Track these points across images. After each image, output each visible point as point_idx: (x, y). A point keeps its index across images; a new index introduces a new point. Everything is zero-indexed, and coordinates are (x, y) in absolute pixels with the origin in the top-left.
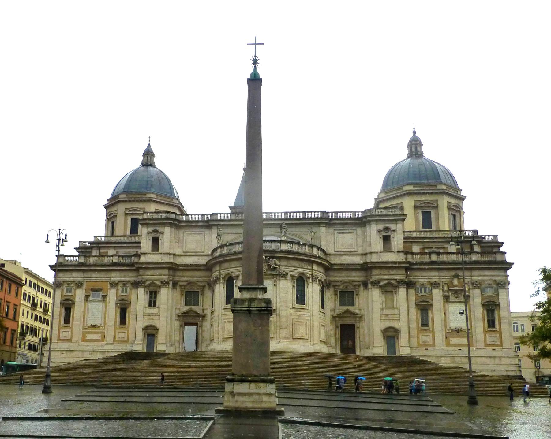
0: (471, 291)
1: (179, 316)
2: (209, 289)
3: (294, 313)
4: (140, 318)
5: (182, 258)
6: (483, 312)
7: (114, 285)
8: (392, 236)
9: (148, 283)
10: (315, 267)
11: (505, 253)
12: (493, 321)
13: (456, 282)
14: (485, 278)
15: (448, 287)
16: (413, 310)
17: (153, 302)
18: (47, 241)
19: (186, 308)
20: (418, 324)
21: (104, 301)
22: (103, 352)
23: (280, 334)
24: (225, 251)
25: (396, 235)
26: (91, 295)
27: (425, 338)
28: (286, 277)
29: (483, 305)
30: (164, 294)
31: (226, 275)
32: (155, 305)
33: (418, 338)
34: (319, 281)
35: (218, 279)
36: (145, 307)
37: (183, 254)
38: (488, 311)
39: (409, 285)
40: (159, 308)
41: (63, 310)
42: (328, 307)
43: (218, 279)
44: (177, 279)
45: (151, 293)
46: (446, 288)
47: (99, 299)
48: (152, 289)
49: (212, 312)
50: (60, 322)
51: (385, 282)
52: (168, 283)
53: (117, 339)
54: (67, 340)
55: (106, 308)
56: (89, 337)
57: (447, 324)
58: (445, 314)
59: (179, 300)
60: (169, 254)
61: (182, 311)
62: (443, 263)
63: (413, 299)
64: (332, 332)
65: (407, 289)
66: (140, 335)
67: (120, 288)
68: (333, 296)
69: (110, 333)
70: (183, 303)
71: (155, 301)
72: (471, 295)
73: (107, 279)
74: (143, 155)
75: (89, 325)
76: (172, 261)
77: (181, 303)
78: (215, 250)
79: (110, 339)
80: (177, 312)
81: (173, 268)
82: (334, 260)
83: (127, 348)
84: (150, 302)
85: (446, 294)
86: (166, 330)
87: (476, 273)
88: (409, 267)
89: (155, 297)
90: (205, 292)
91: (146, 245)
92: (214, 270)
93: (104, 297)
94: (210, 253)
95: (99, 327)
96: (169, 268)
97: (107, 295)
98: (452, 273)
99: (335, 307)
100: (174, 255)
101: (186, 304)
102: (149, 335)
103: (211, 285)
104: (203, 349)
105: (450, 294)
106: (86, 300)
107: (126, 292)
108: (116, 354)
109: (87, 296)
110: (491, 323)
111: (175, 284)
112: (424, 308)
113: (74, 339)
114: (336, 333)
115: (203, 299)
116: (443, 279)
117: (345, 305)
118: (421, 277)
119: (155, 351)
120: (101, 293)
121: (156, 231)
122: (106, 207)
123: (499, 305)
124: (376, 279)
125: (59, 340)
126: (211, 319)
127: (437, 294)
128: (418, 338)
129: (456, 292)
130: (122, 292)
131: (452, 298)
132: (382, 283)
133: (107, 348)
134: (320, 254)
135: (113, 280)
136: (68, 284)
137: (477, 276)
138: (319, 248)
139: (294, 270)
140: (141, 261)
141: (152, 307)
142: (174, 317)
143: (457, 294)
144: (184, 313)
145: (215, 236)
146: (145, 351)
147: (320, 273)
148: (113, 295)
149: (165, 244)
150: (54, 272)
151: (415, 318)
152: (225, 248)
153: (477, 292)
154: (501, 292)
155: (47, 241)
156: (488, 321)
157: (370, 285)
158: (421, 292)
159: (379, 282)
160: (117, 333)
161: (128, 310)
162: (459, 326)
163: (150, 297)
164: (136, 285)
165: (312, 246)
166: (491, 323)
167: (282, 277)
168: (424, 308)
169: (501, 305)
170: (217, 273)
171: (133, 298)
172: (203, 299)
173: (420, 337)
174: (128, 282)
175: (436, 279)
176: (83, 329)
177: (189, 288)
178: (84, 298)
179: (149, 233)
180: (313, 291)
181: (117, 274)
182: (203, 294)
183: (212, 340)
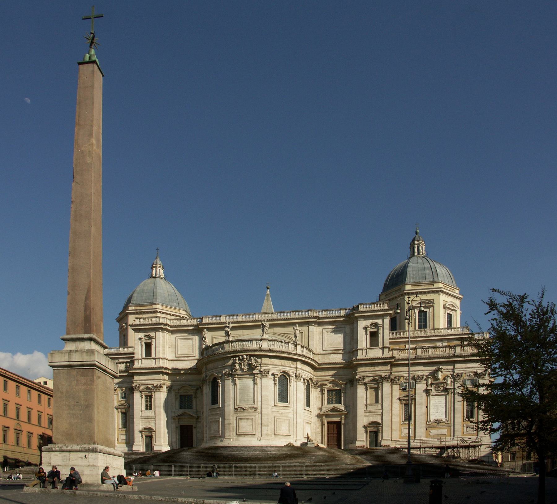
10: (299, 365)
14: (467, 370)
19: (181, 411)
34: (304, 379)
39: (393, 381)
42: (315, 406)
45: (146, 396)
51: (371, 378)
61: (176, 415)
64: (319, 430)
70: (178, 406)
71: (151, 405)
77: (175, 406)
82: (320, 359)
85: (429, 388)
87: (457, 366)
88: (392, 363)
89: (151, 401)
99: (322, 405)
101: (181, 408)
117: (332, 403)
121: (149, 337)
124: (362, 375)
132: (367, 380)
134: (305, 352)
139: (276, 367)
147: (306, 372)
157: (355, 382)
159: (364, 379)
162: (439, 418)
163: (147, 401)
165: (296, 345)
168: (408, 403)
177: (182, 392)
182: (196, 397)
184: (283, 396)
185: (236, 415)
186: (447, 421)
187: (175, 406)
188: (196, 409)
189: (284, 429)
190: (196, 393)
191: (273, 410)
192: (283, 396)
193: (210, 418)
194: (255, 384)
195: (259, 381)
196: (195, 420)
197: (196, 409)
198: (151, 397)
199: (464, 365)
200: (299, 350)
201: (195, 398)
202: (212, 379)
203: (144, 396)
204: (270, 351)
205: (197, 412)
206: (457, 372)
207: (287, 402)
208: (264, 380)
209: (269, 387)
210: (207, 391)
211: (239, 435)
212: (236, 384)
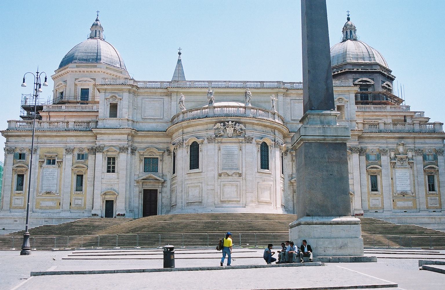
1: (138, 182)
2: (169, 154)
3: (259, 177)
5: (141, 124)
6: (425, 178)
7: (69, 151)
11: (443, 124)
12: (433, 186)
13: (401, 149)
15: (395, 154)
17: (111, 168)
20: (368, 190)
22: (60, 219)
23: (246, 197)
25: (349, 105)
28: (251, 143)
29: (425, 171)
32: (113, 171)
33: (369, 201)
35: (181, 144)
37: (142, 121)
38: (429, 177)
39: (361, 151)
44: (136, 145)
45: (109, 159)
46: (393, 155)
48: (111, 154)
52: (127, 149)
53: (73, 205)
54: (21, 208)
57: (395, 188)
59: (138, 167)
61: (141, 178)
63: (364, 164)
65: (359, 155)
68: (291, 163)
70: (142, 169)
71: (114, 167)
73: (62, 145)
77: (140, 169)
79: (66, 206)
80: (136, 177)
84: (109, 168)
86: (126, 197)
87: (417, 141)
89: (114, 163)
90: (164, 159)
91: (104, 110)
92: (174, 136)
97: (62, 162)
98: (397, 141)
99: (292, 173)
106: (41, 167)
111: (133, 151)
114: (293, 197)
115: (162, 165)
116: (391, 146)
126: (171, 185)
128: (369, 201)
129: (402, 159)
131: (398, 163)
133: (63, 215)
140: (97, 127)
141: (111, 174)
142: (134, 184)
144: (143, 179)
145: (174, 103)
149: (123, 111)
150: (5, 139)
156: (429, 185)
160: (73, 200)
161: (84, 177)
163: (109, 163)
164: (94, 150)
166: (432, 188)
167: (248, 142)
170: (180, 138)
172: (162, 165)
173: (370, 200)
174: (84, 148)
175: (384, 146)
176: (38, 196)
180: (275, 158)
181: (74, 139)
182: (162, 160)
183: (173, 206)
185: (219, 180)
186: (413, 193)
187: (140, 169)
188: (162, 173)
190: (162, 156)
192: (265, 164)
193: (188, 182)
196: (161, 184)
197: (162, 173)
198: (114, 159)
199: (422, 141)
201: (161, 160)
202: (190, 144)
203: (107, 158)
205: (163, 175)
208: (248, 146)
209: (253, 151)
210: (183, 156)
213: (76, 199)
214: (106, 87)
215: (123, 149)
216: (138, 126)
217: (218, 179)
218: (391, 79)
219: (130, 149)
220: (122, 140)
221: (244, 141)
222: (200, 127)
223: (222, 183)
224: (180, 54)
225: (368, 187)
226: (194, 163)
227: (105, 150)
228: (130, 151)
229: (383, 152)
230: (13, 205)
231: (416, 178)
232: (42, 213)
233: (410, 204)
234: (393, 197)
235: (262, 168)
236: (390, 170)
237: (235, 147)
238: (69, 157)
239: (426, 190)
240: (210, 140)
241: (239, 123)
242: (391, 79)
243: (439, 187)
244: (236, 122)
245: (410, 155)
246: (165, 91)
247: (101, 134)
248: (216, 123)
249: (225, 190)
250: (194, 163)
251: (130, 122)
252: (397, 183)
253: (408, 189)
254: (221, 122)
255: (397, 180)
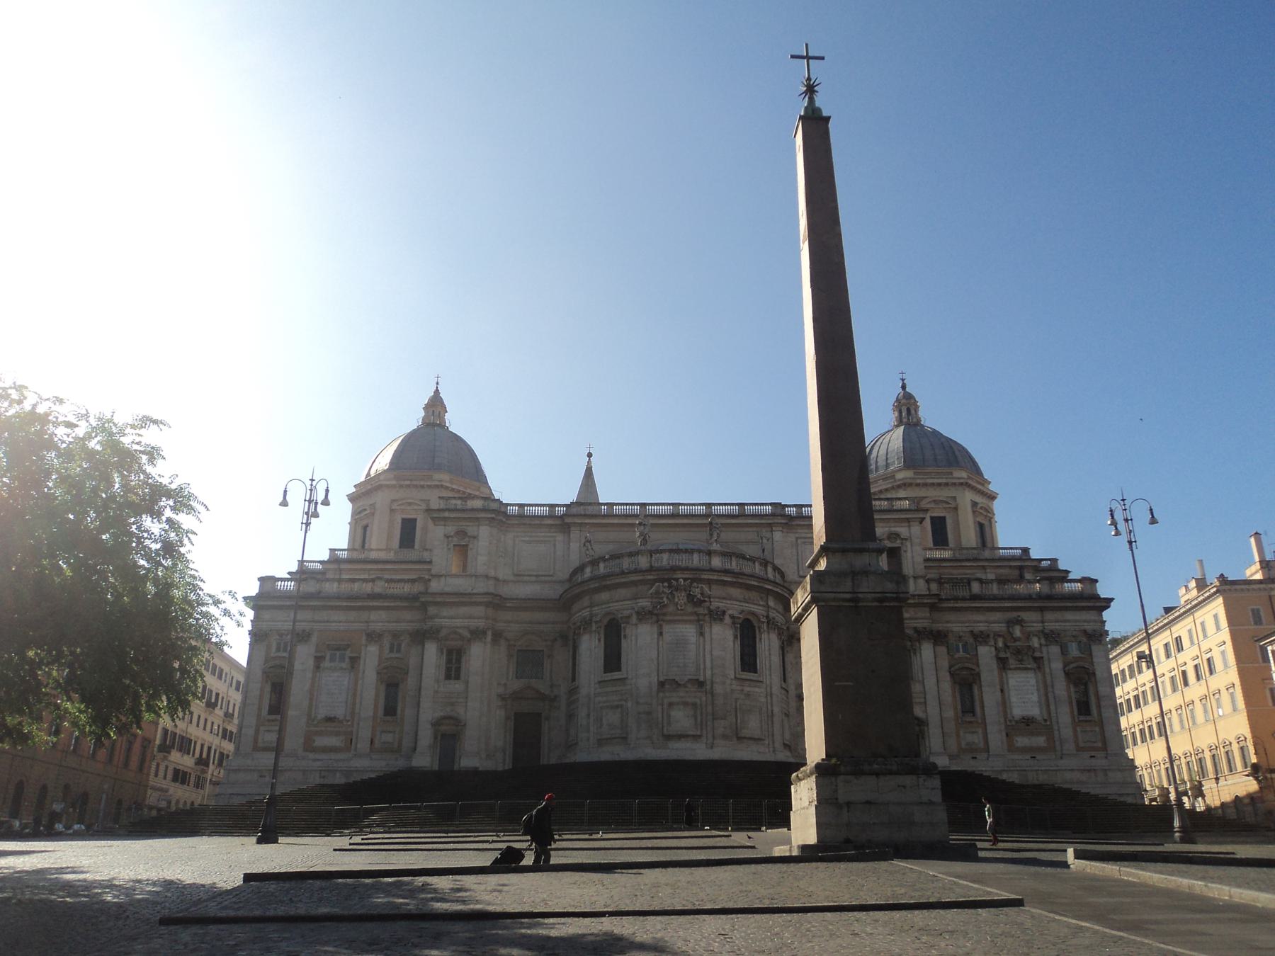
0: (1044, 649)
4: (426, 704)
7: (373, 637)
8: (904, 548)
9: (444, 633)
11: (1096, 581)
13: (1017, 632)
16: (947, 685)
18: (284, 503)
19: (516, 685)
21: (353, 667)
24: (602, 569)
26: (328, 658)
27: (969, 738)
29: (1067, 674)
30: (478, 657)
31: (608, 614)
32: (457, 677)
33: (958, 736)
35: (587, 623)
36: (437, 681)
37: (512, 578)
39: (938, 637)
40: (467, 682)
41: (268, 688)
43: (587, 623)
45: (450, 652)
46: (1000, 644)
47: (344, 665)
49: (573, 691)
50: (260, 709)
52: (484, 633)
53: (377, 744)
55: (356, 684)
56: (320, 741)
58: (1002, 691)
60: (487, 577)
62: (995, 598)
63: (945, 664)
65: (935, 645)
66: (426, 737)
67: (386, 642)
69: (365, 733)
71: (458, 670)
72: (1045, 655)
74: (426, 408)
75: (319, 717)
76: (492, 590)
78: (581, 569)
79: (363, 746)
80: (501, 690)
81: (497, 602)
83: (398, 764)
84: (448, 670)
85: (1002, 655)
87: (1049, 616)
89: (459, 661)
91: (443, 559)
92: (576, 607)
93: (354, 661)
94: (567, 576)
95: (341, 722)
96: (487, 605)
97: (358, 658)
100: (496, 579)
102: (443, 736)
103: (569, 640)
104: (553, 761)
105: (1008, 655)
106: (317, 667)
107: (399, 651)
108: (373, 776)
109: (319, 659)
110: (1083, 707)
111: (497, 636)
112: (966, 682)
113: (288, 745)
116: (997, 627)
118: (957, 624)
119: (456, 768)
120: (348, 653)
121: (461, 533)
122: (352, 498)
123: (1094, 674)
125: (256, 748)
127: (985, 653)
128: (958, 736)
129: (1018, 652)
130: (391, 651)
135: (373, 627)
136: (281, 635)
137: (1054, 621)
138: (775, 568)
141: (452, 682)
143: (1017, 655)
145: (575, 546)
146: (436, 767)
148: (371, 656)
151: (950, 699)
152: (602, 565)
153: (1055, 649)
154: (1095, 648)
155: (284, 503)
156: (1078, 703)
158: (958, 651)
163: (449, 661)
164: (420, 637)
165: (765, 563)
169: (1098, 673)
170: (586, 613)
171: (413, 662)
175: (982, 627)
178: (311, 662)
179: (447, 537)
181: (383, 615)
184: (749, 661)
189: (753, 725)
191: (734, 687)
192: (749, 661)
194: (702, 634)
195: (707, 629)
199: (1058, 615)
200: (770, 574)
202: (605, 621)
204: (726, 572)
205: (552, 686)
206: (1050, 626)
207: (755, 671)
210: (591, 648)
211: (669, 737)
212: (661, 634)
213: (383, 732)
214: (446, 514)
215: (477, 634)
216: (506, 591)
217: (658, 691)
218: (992, 497)
219: (489, 633)
220: (475, 616)
221: (707, 618)
222: (623, 592)
223: (666, 701)
224: (590, 455)
225: (955, 708)
226: (613, 660)
227: (444, 633)
228: (489, 638)
229: (981, 638)
230: (260, 744)
231: (1050, 689)
232: (315, 760)
233: (1041, 741)
234: (1007, 726)
235: (743, 670)
236: (996, 673)
237: (689, 631)
238: (373, 649)
239: (1072, 712)
240: (643, 615)
241: (700, 581)
242: (992, 497)
243: (1099, 707)
244: (693, 580)
245: (1035, 642)
246: (558, 522)
247: (436, 604)
248: (655, 581)
249: (673, 713)
250: (613, 660)
251: (491, 582)
252: (1013, 699)
253: (1035, 711)
254: (663, 580)
255: (1013, 693)
